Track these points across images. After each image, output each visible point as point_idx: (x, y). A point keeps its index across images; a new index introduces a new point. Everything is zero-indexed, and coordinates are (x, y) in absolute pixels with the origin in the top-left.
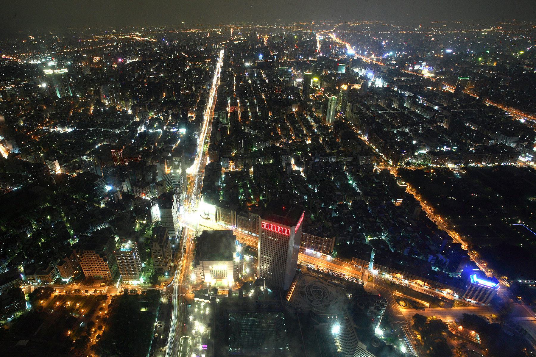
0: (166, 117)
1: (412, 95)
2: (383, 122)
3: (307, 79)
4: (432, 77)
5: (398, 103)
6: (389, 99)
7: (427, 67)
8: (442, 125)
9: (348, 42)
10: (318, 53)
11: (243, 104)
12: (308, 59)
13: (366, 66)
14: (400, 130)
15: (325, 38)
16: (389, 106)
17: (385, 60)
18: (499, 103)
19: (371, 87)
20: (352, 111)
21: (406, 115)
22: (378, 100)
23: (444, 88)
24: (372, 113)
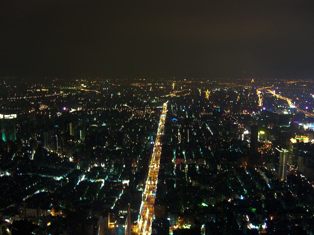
9: (289, 98)
10: (262, 107)
11: (189, 156)
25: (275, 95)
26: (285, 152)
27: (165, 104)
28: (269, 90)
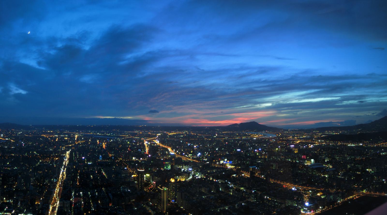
0: (16, 202)
3: (141, 175)
4: (234, 168)
7: (228, 161)
8: (249, 200)
9: (170, 146)
10: (148, 155)
12: (140, 159)
13: (187, 163)
14: (222, 208)
15: (151, 143)
17: (198, 159)
18: (278, 180)
23: (243, 175)
25: (159, 144)
26: (165, 189)
27: (68, 152)
28: (154, 141)
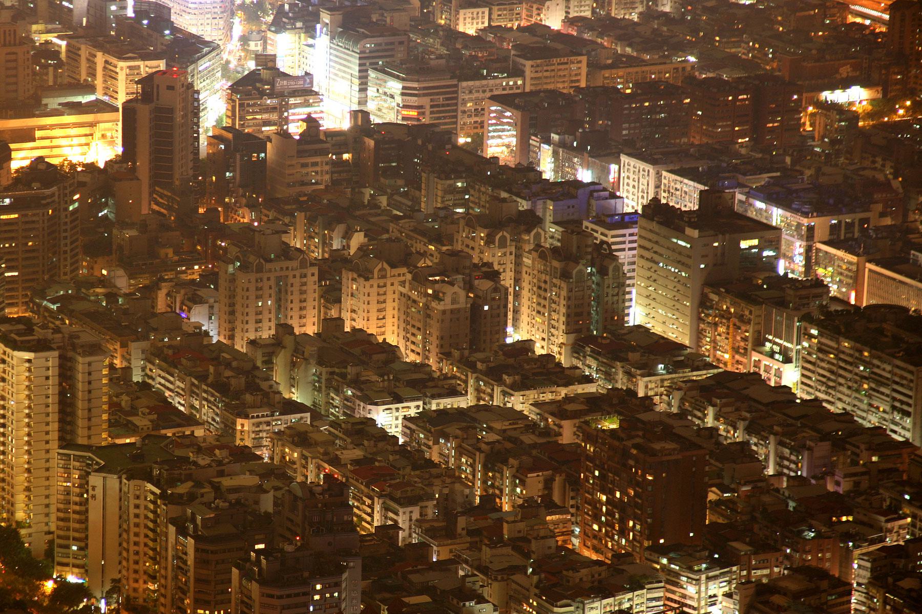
1: (686, 194)
2: (442, 530)
5: (559, 293)
6: (456, 266)
16: (475, 338)
19: (238, 142)
20: (67, 440)
21: (666, 428)
22: (332, 275)
24: (299, 438)
